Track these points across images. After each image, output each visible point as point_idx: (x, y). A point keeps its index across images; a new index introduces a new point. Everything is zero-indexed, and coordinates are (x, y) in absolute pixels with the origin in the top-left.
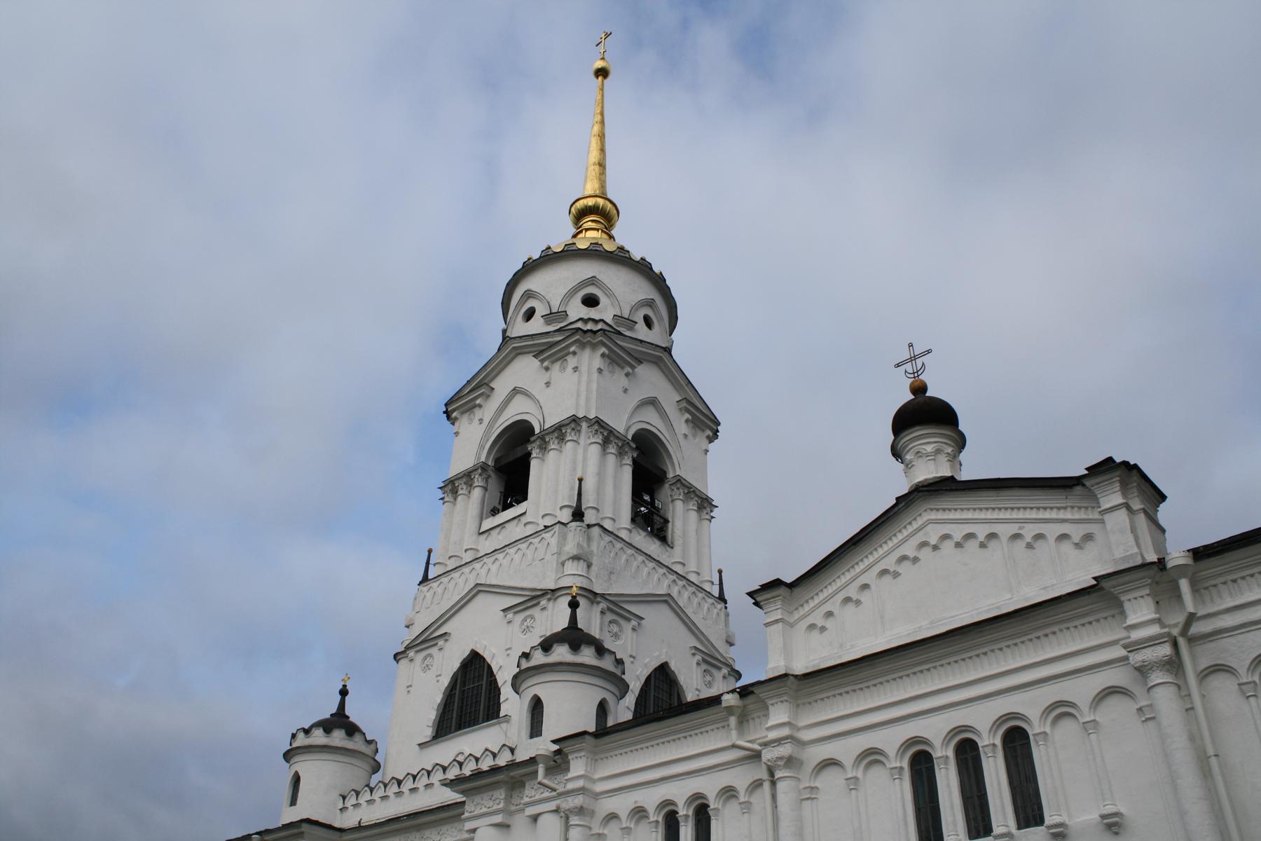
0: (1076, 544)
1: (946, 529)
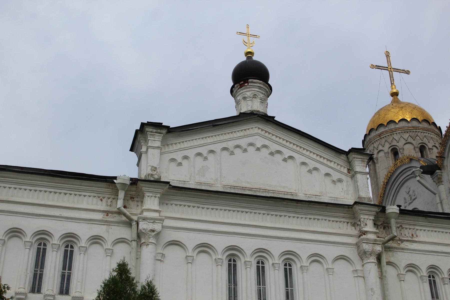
0: (334, 181)
1: (267, 142)
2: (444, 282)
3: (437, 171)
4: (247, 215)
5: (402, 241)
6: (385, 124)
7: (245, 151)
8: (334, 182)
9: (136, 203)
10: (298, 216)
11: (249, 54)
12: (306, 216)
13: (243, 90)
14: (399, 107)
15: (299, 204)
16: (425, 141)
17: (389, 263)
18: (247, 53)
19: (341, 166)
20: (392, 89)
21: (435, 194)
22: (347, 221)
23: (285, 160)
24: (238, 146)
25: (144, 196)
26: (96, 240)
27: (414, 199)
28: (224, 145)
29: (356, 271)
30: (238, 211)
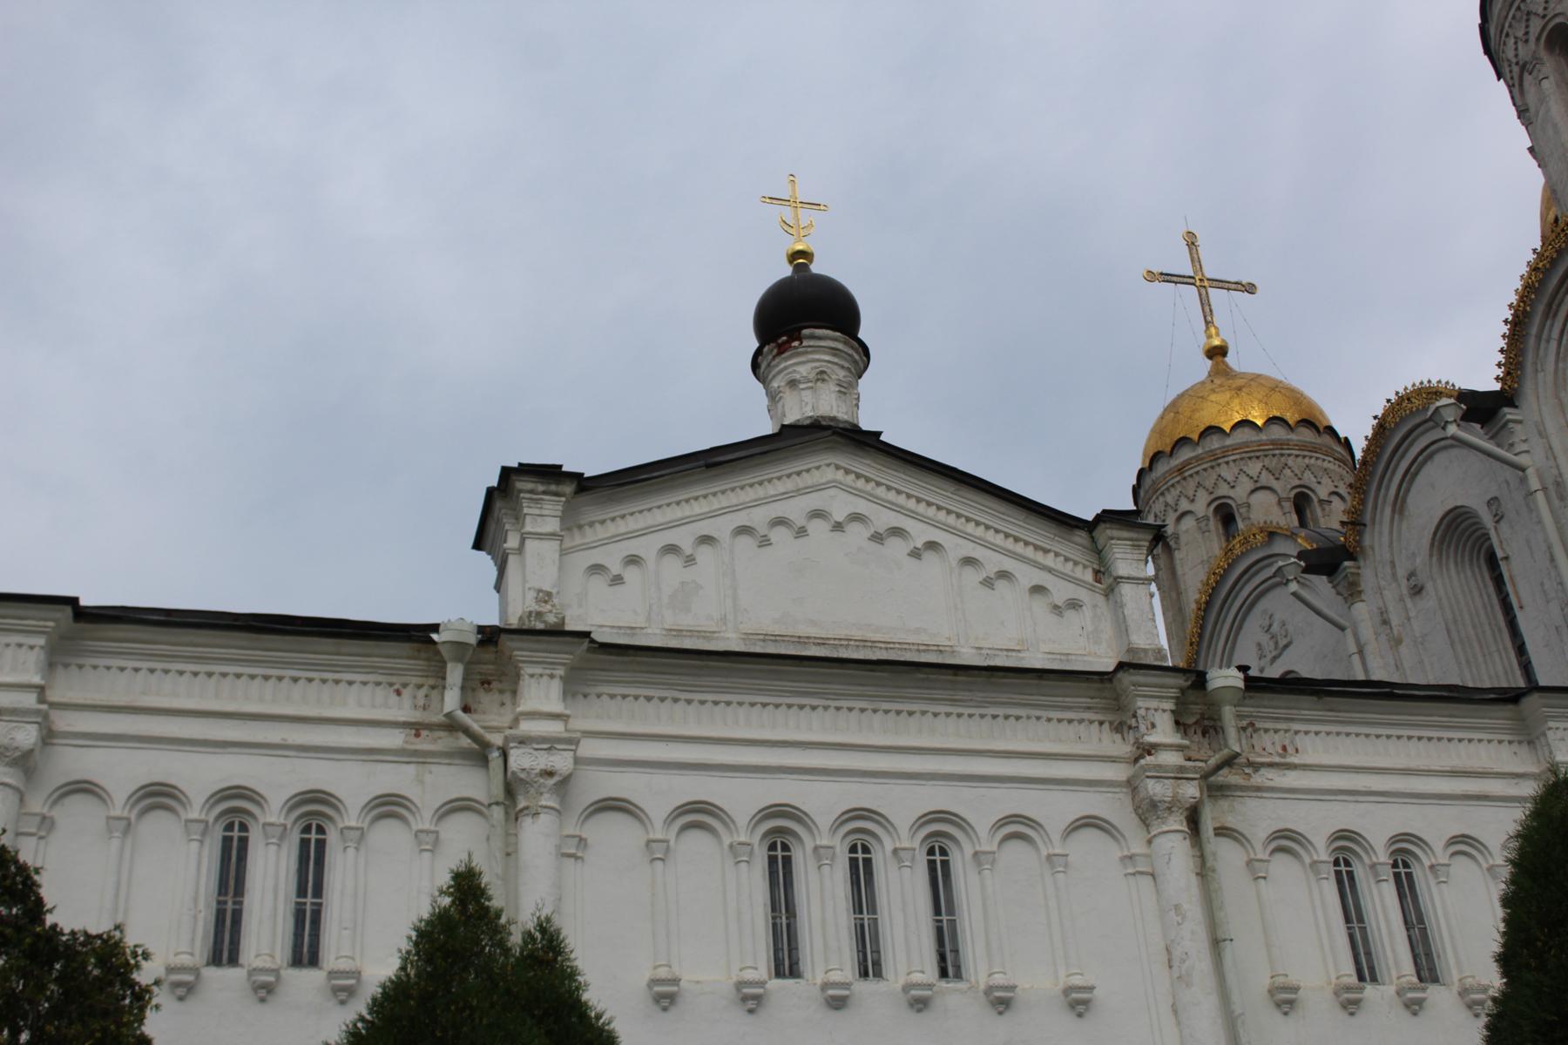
0: (1056, 607)
1: (862, 506)
2: (1376, 874)
3: (1346, 563)
4: (814, 715)
5: (1257, 767)
6: (1195, 437)
7: (802, 532)
8: (1056, 608)
9: (496, 697)
10: (960, 710)
11: (800, 258)
12: (983, 711)
13: (786, 359)
14: (1230, 388)
15: (961, 678)
16: (1309, 479)
17: (1222, 831)
18: (794, 256)
19: (1076, 563)
20: (1209, 337)
21: (1343, 629)
22: (1100, 717)
23: (915, 554)
24: (780, 522)
25: (518, 676)
26: (389, 807)
27: (1286, 646)
28: (741, 519)
29: (1131, 857)
30: (790, 706)
